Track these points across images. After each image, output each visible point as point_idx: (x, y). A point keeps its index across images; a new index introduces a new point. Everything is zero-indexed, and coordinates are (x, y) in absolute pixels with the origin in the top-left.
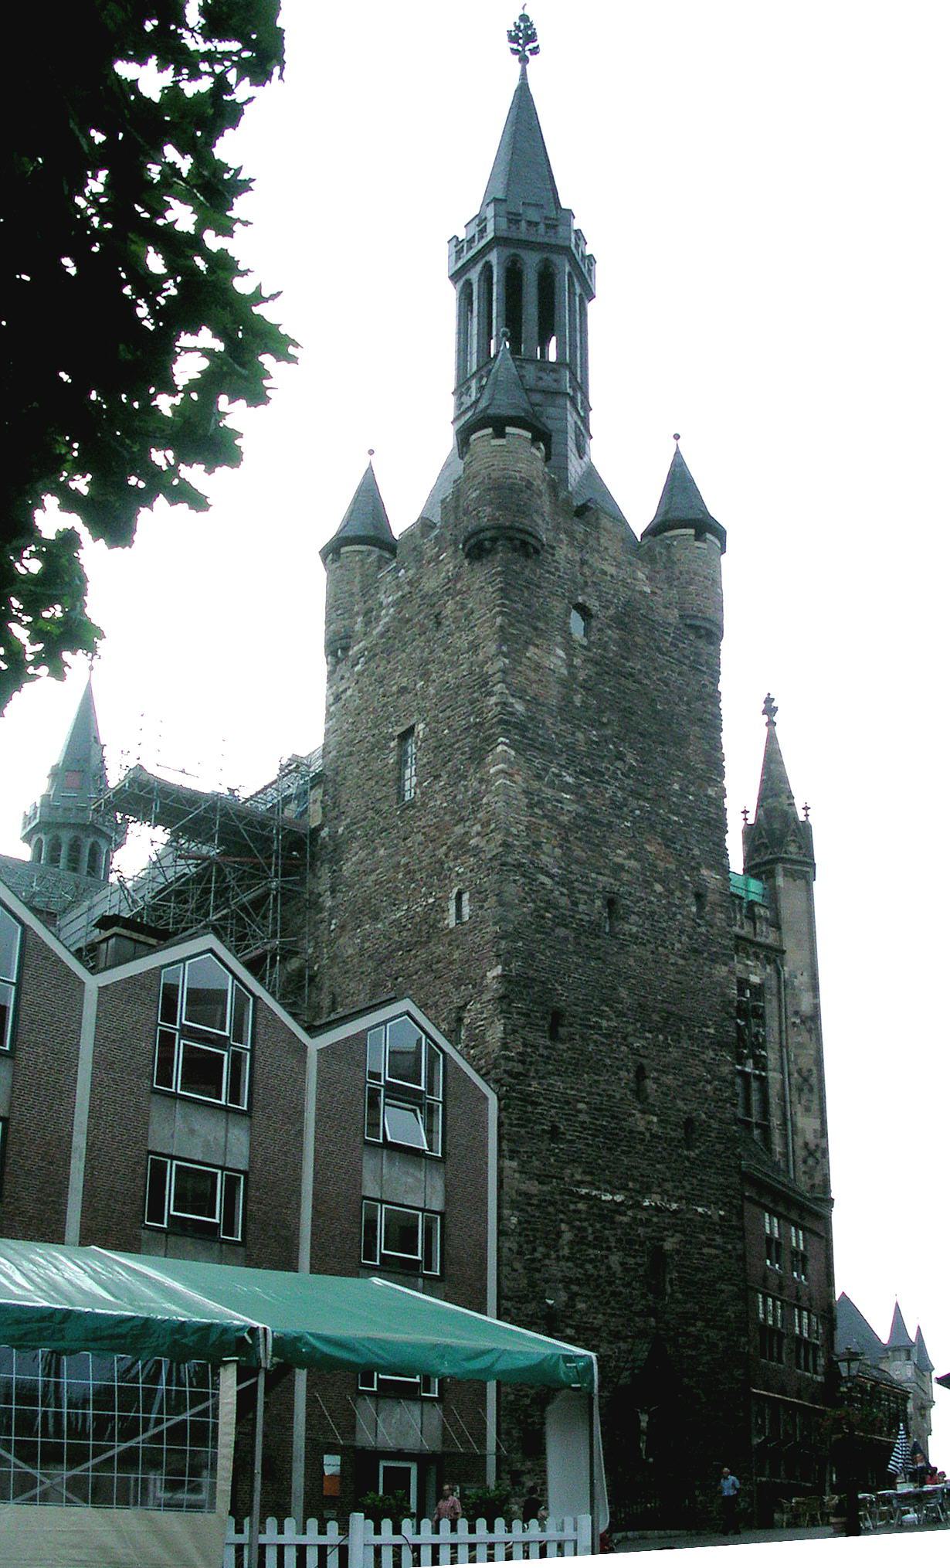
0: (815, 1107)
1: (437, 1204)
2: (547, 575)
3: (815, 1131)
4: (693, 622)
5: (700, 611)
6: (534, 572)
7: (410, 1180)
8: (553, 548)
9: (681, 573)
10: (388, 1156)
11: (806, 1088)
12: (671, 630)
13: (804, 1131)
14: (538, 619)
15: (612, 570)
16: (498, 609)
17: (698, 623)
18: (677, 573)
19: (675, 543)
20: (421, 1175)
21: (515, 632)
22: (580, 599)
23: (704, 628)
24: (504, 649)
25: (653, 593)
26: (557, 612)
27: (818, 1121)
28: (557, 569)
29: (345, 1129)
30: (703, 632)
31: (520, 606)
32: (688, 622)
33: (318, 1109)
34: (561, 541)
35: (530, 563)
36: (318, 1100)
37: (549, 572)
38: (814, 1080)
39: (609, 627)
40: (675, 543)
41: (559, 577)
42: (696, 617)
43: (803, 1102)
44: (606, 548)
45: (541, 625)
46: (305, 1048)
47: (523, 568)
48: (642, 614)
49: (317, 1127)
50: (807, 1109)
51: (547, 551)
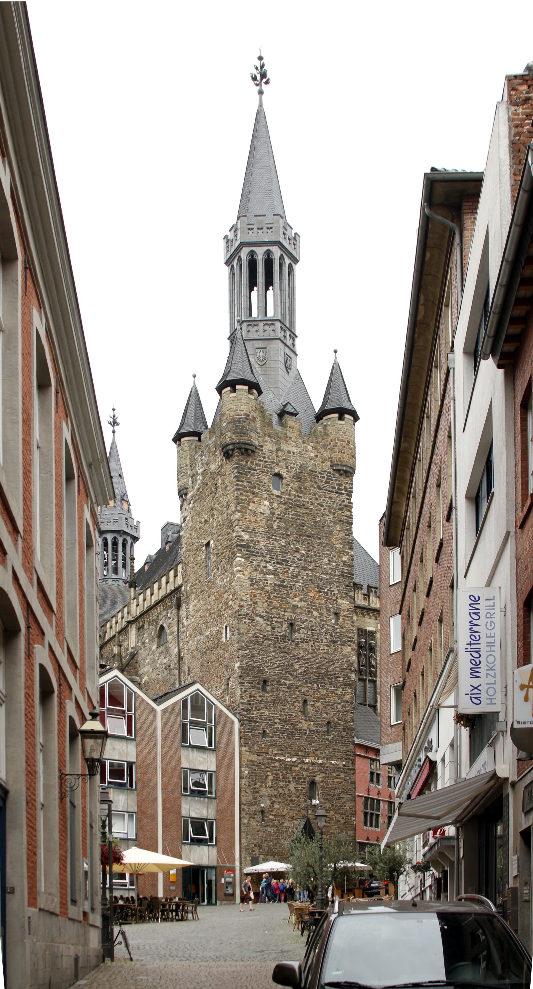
2: (259, 462)
4: (337, 468)
5: (340, 461)
6: (252, 463)
8: (262, 446)
9: (331, 441)
12: (325, 475)
14: (255, 488)
15: (294, 450)
16: (235, 487)
17: (340, 468)
18: (329, 440)
19: (329, 423)
21: (243, 498)
22: (277, 471)
23: (343, 470)
24: (238, 508)
25: (316, 456)
26: (264, 482)
28: (264, 457)
30: (342, 472)
31: (245, 483)
32: (335, 468)
34: (266, 442)
35: (251, 459)
37: (260, 460)
39: (292, 481)
40: (329, 423)
41: (266, 462)
42: (338, 465)
44: (291, 438)
45: (256, 491)
47: (247, 462)
48: (310, 470)
51: (259, 449)
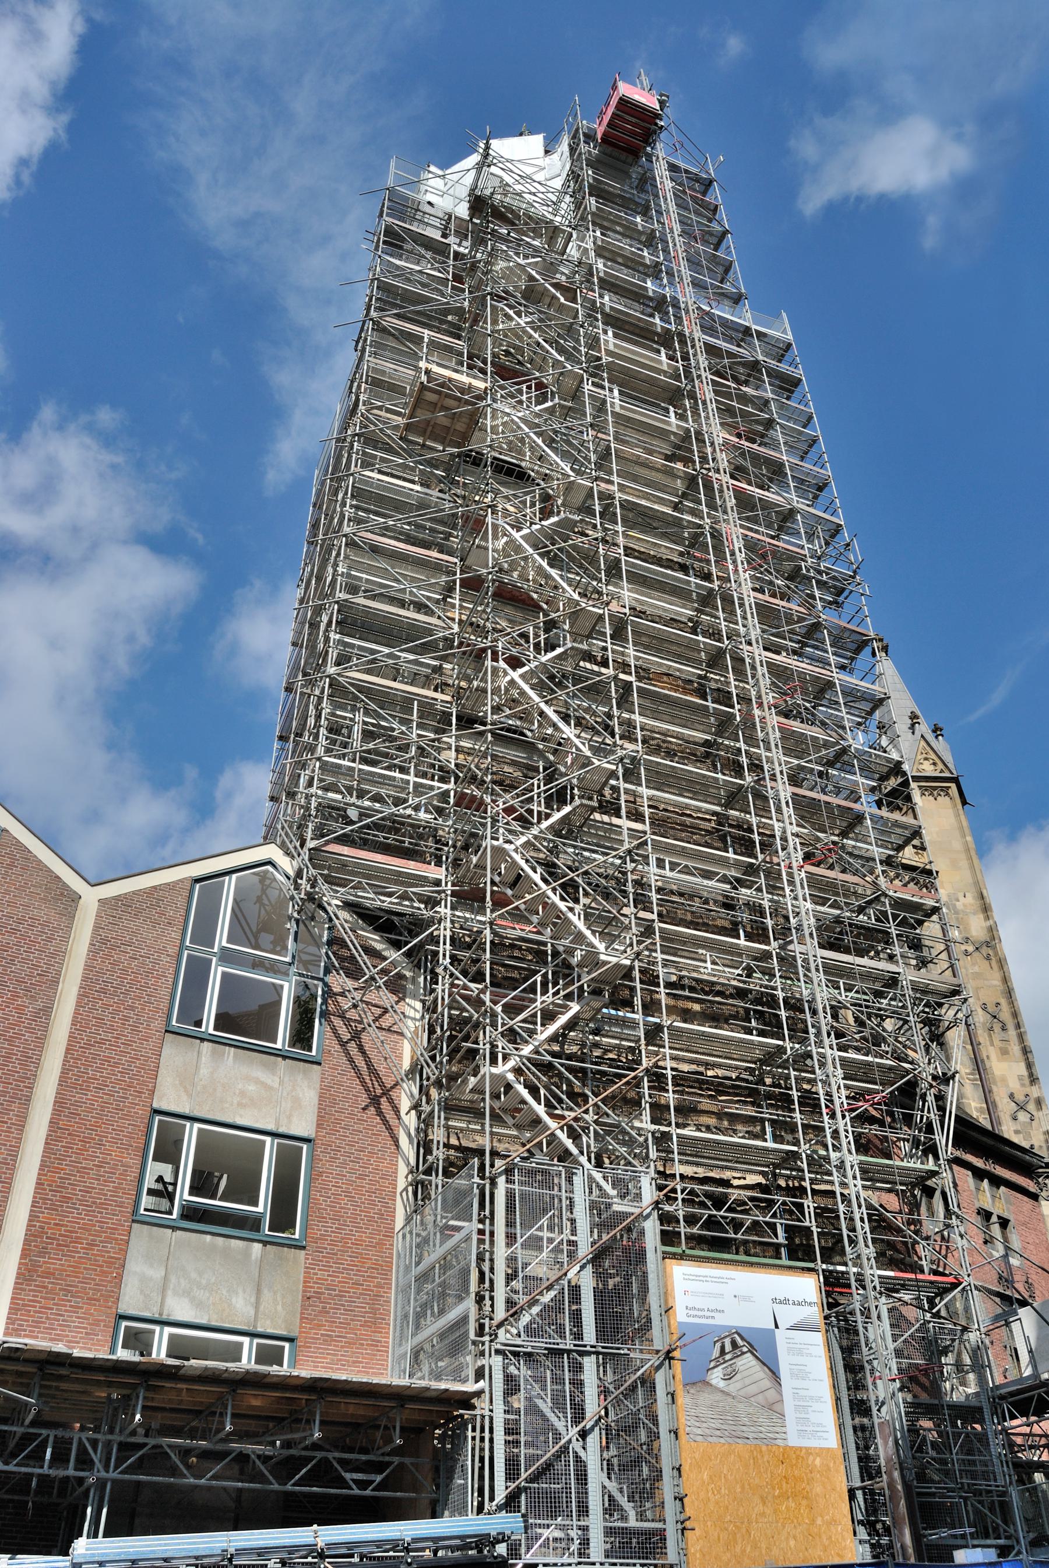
0: (1016, 1049)
1: (303, 1125)
3: (1020, 1078)
7: (252, 1088)
10: (214, 1052)
11: (997, 1027)
13: (1004, 1079)
20: (272, 1080)
27: (1022, 1066)
29: (132, 1008)
33: (85, 978)
36: (88, 968)
38: (1005, 1015)
43: (997, 1042)
46: (75, 898)
49: (79, 1004)
50: (1004, 1052)
